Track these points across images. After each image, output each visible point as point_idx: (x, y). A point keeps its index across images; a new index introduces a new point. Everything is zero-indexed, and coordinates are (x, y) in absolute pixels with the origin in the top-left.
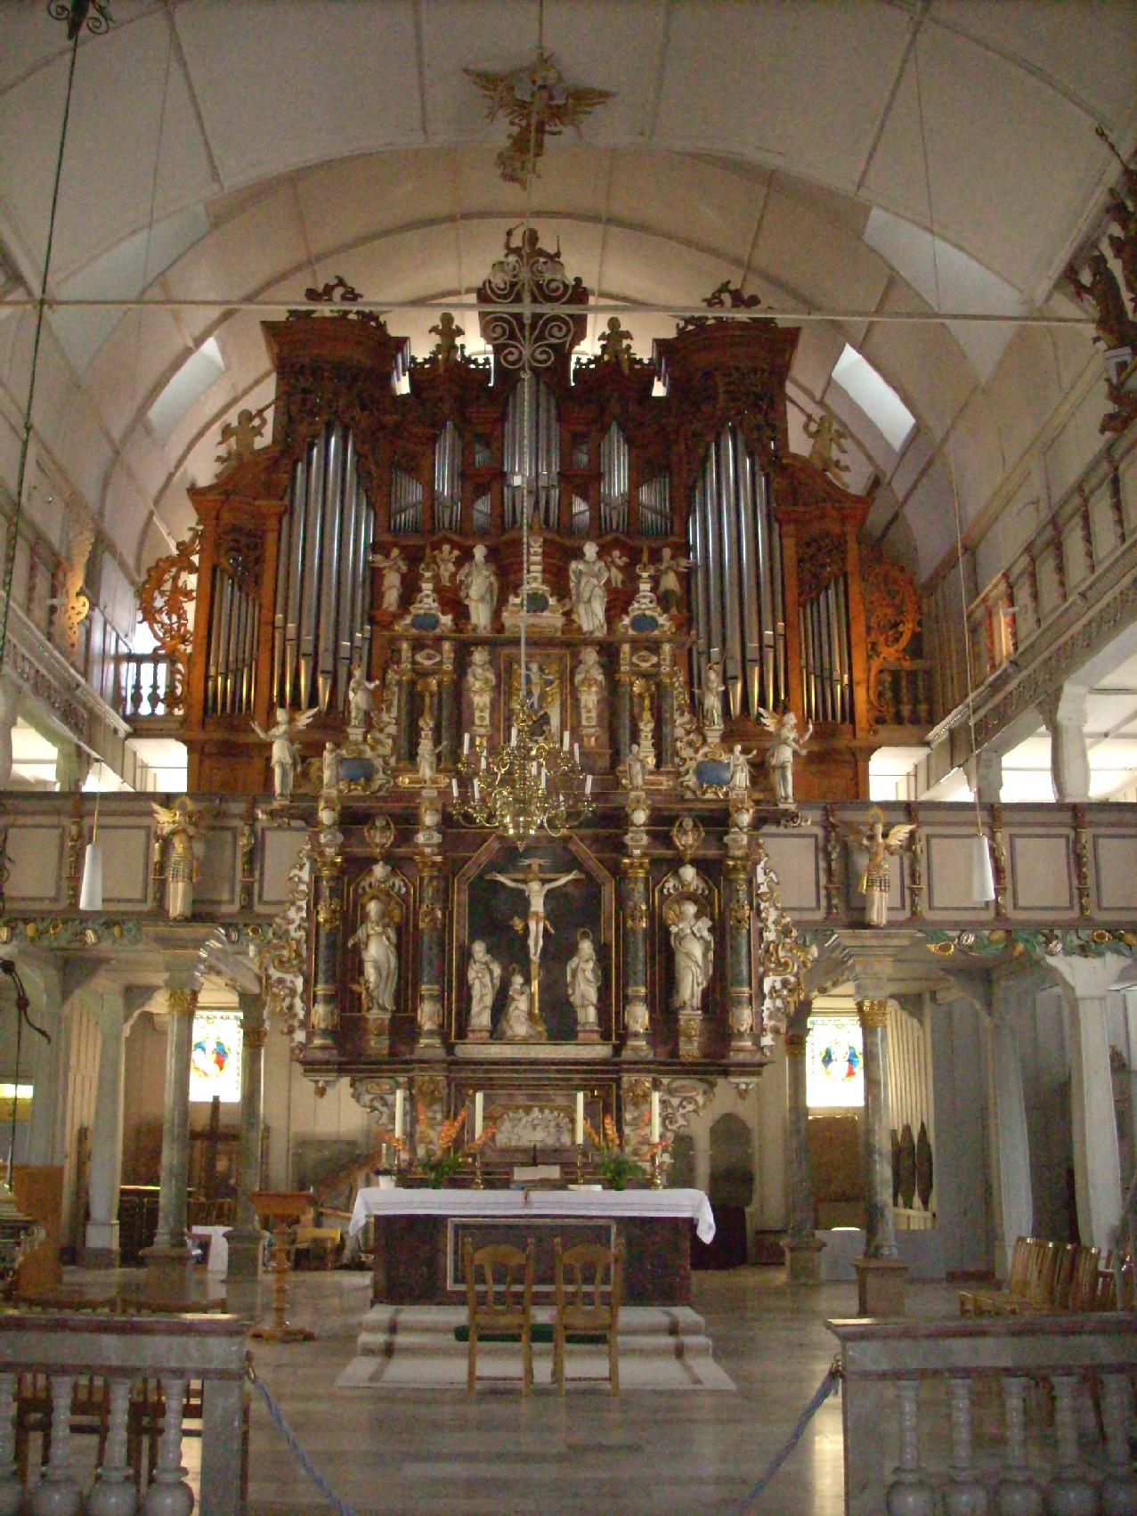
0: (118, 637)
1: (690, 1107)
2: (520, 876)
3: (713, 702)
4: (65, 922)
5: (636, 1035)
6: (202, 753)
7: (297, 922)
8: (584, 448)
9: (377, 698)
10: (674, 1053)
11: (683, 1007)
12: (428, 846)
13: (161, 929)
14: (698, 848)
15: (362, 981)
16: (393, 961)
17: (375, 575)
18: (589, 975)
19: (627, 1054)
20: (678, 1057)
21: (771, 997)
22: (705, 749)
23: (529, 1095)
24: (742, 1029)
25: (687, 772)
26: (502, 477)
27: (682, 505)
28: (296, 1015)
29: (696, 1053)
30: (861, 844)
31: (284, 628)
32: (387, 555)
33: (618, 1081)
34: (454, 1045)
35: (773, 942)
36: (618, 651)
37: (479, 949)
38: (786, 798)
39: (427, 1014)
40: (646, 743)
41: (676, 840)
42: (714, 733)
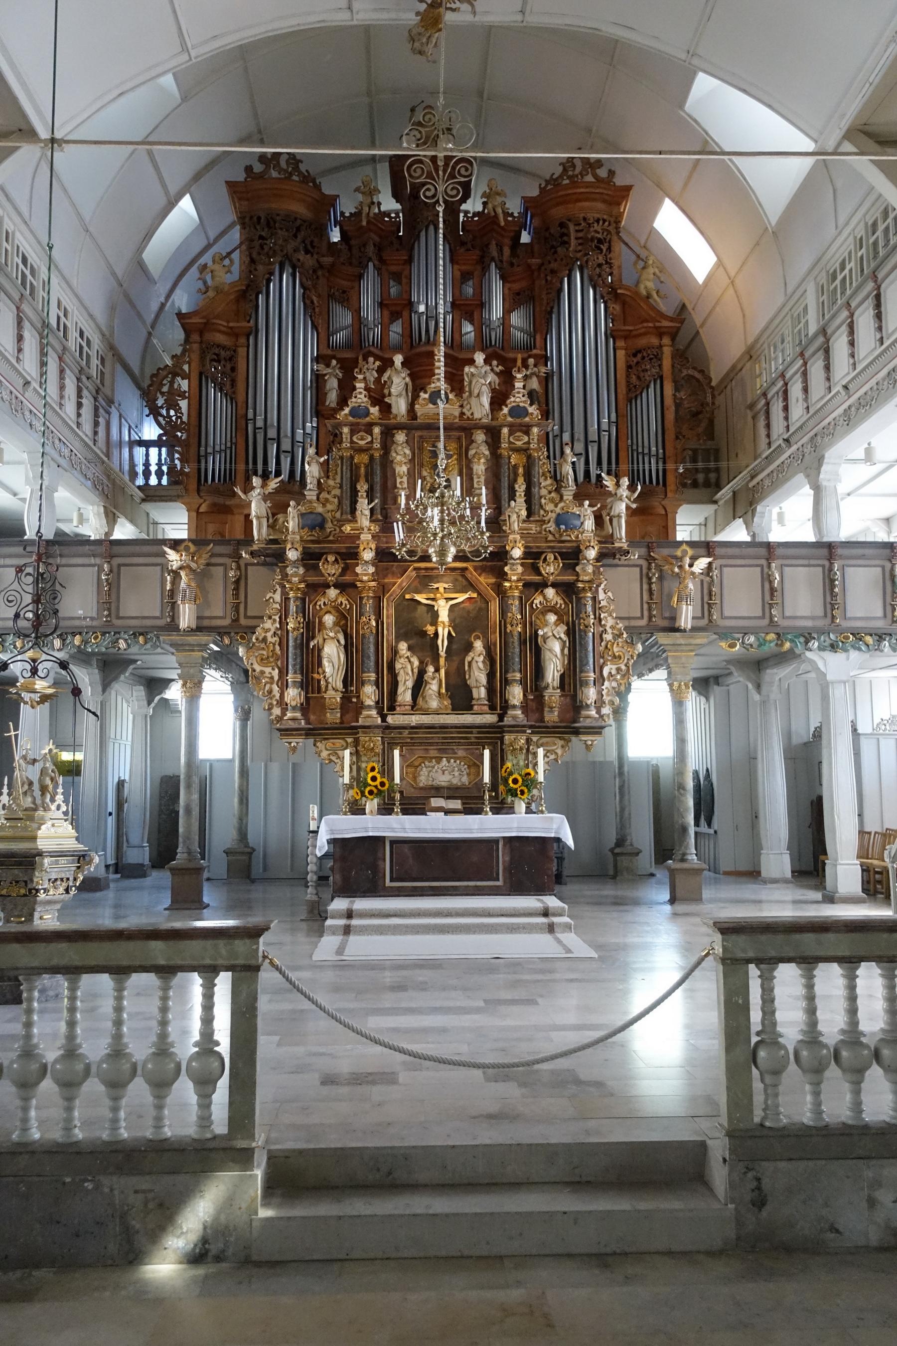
0: (130, 427)
1: (552, 757)
2: (432, 596)
3: (568, 469)
4: (103, 634)
5: (514, 707)
7: (273, 630)
8: (471, 283)
9: (325, 467)
10: (542, 720)
11: (547, 687)
12: (366, 575)
13: (175, 638)
14: (557, 575)
15: (320, 670)
16: (342, 656)
18: (481, 665)
19: (507, 721)
20: (544, 722)
21: (609, 680)
22: (561, 505)
23: (439, 749)
24: (589, 702)
25: (549, 522)
26: (410, 305)
28: (274, 696)
29: (556, 719)
30: (673, 572)
31: (255, 419)
33: (502, 739)
34: (386, 715)
35: (610, 641)
36: (499, 432)
37: (403, 646)
38: (621, 539)
39: (369, 694)
40: (521, 499)
41: (541, 569)
42: (568, 495)
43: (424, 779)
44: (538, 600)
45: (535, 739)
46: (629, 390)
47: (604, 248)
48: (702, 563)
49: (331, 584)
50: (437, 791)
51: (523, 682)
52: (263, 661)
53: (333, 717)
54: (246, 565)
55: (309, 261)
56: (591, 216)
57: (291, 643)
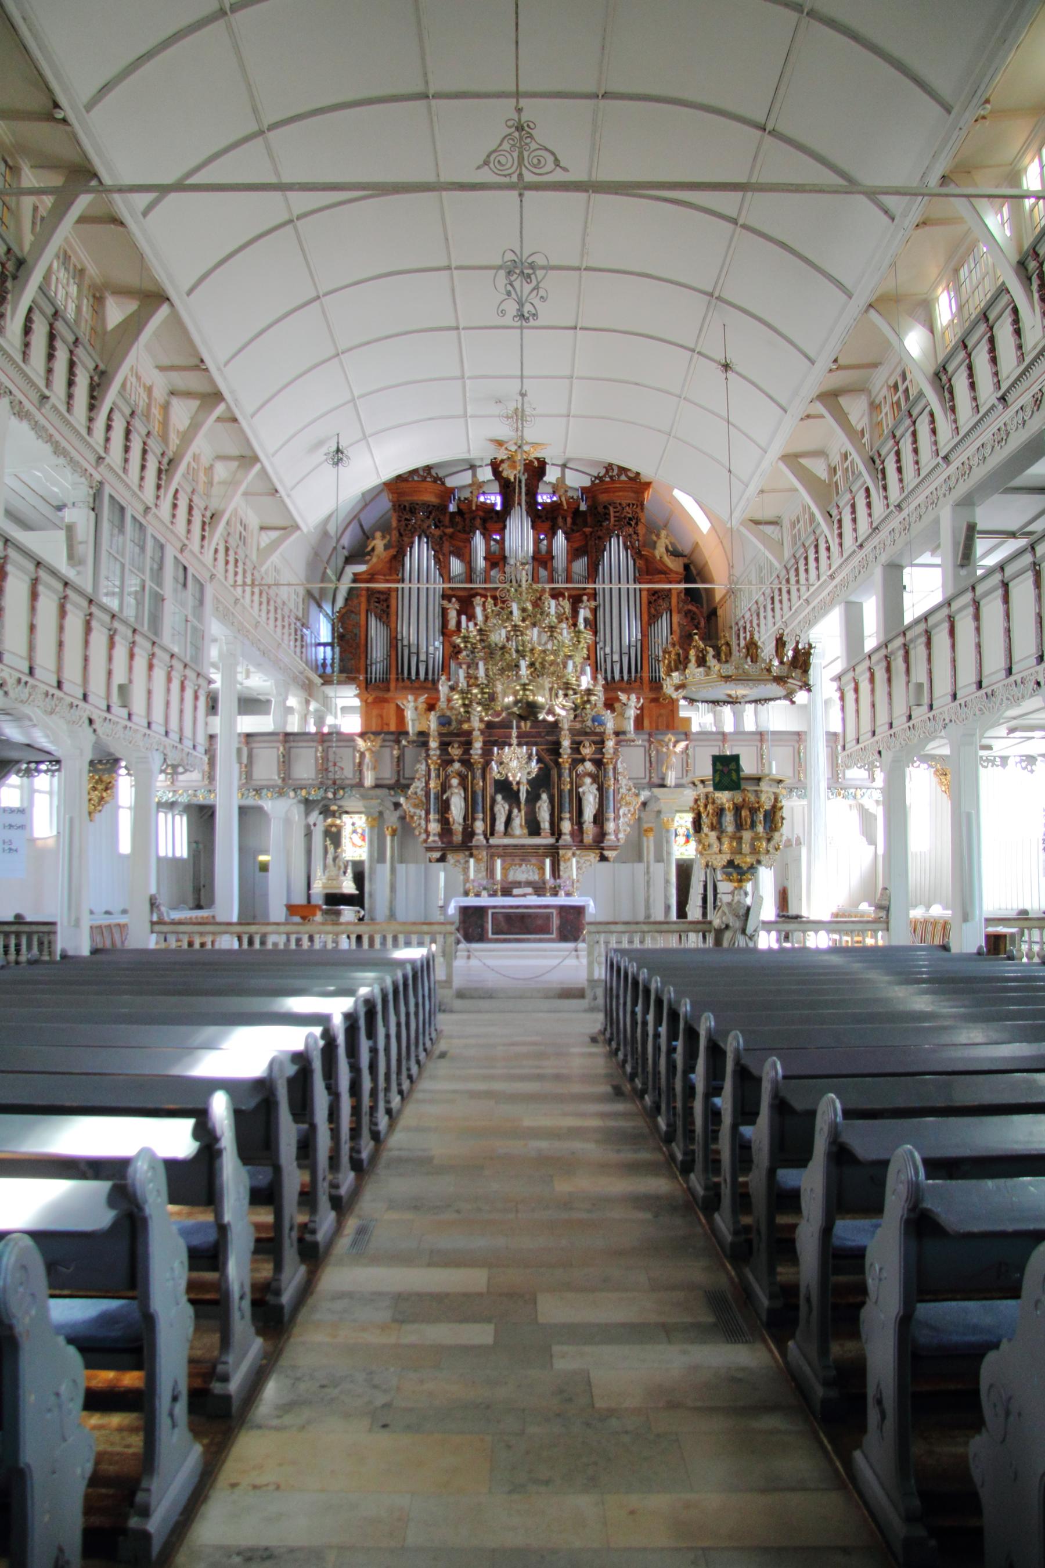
6: (366, 701)
10: (582, 841)
17: (444, 612)
19: (561, 842)
27: (593, 573)
31: (402, 640)
32: (450, 601)
33: (558, 853)
37: (499, 797)
39: (479, 826)
43: (511, 877)
44: (580, 769)
45: (578, 852)
46: (650, 619)
47: (633, 523)
48: (682, 745)
49: (455, 757)
50: (518, 884)
51: (571, 819)
52: (416, 806)
53: (458, 838)
54: (405, 746)
55: (438, 533)
56: (624, 503)
57: (432, 796)
